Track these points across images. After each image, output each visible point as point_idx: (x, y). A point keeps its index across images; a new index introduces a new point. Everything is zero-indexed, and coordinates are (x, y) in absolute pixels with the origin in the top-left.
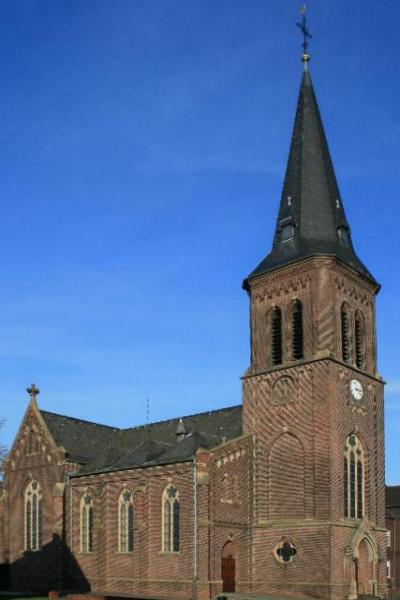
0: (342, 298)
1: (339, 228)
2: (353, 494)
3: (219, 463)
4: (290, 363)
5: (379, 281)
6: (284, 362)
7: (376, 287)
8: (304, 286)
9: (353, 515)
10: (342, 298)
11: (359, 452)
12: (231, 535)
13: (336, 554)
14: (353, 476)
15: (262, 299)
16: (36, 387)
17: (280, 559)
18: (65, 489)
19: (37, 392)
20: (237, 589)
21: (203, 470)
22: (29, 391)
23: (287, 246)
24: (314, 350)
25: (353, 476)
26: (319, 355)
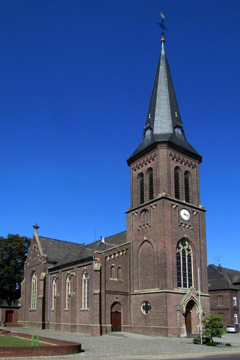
0: (174, 164)
1: (175, 127)
2: (185, 274)
3: (108, 258)
4: (148, 202)
5: (200, 155)
6: (145, 202)
7: (199, 159)
8: (153, 160)
9: (185, 286)
10: (174, 164)
11: (188, 250)
12: (117, 298)
13: (170, 309)
14: (184, 264)
15: (135, 170)
16: (38, 225)
17: (144, 313)
18: (45, 277)
19: (38, 227)
20: (122, 329)
21: (98, 262)
22: (38, 227)
23: (147, 140)
24: (158, 193)
25: (184, 264)
26: (160, 196)
